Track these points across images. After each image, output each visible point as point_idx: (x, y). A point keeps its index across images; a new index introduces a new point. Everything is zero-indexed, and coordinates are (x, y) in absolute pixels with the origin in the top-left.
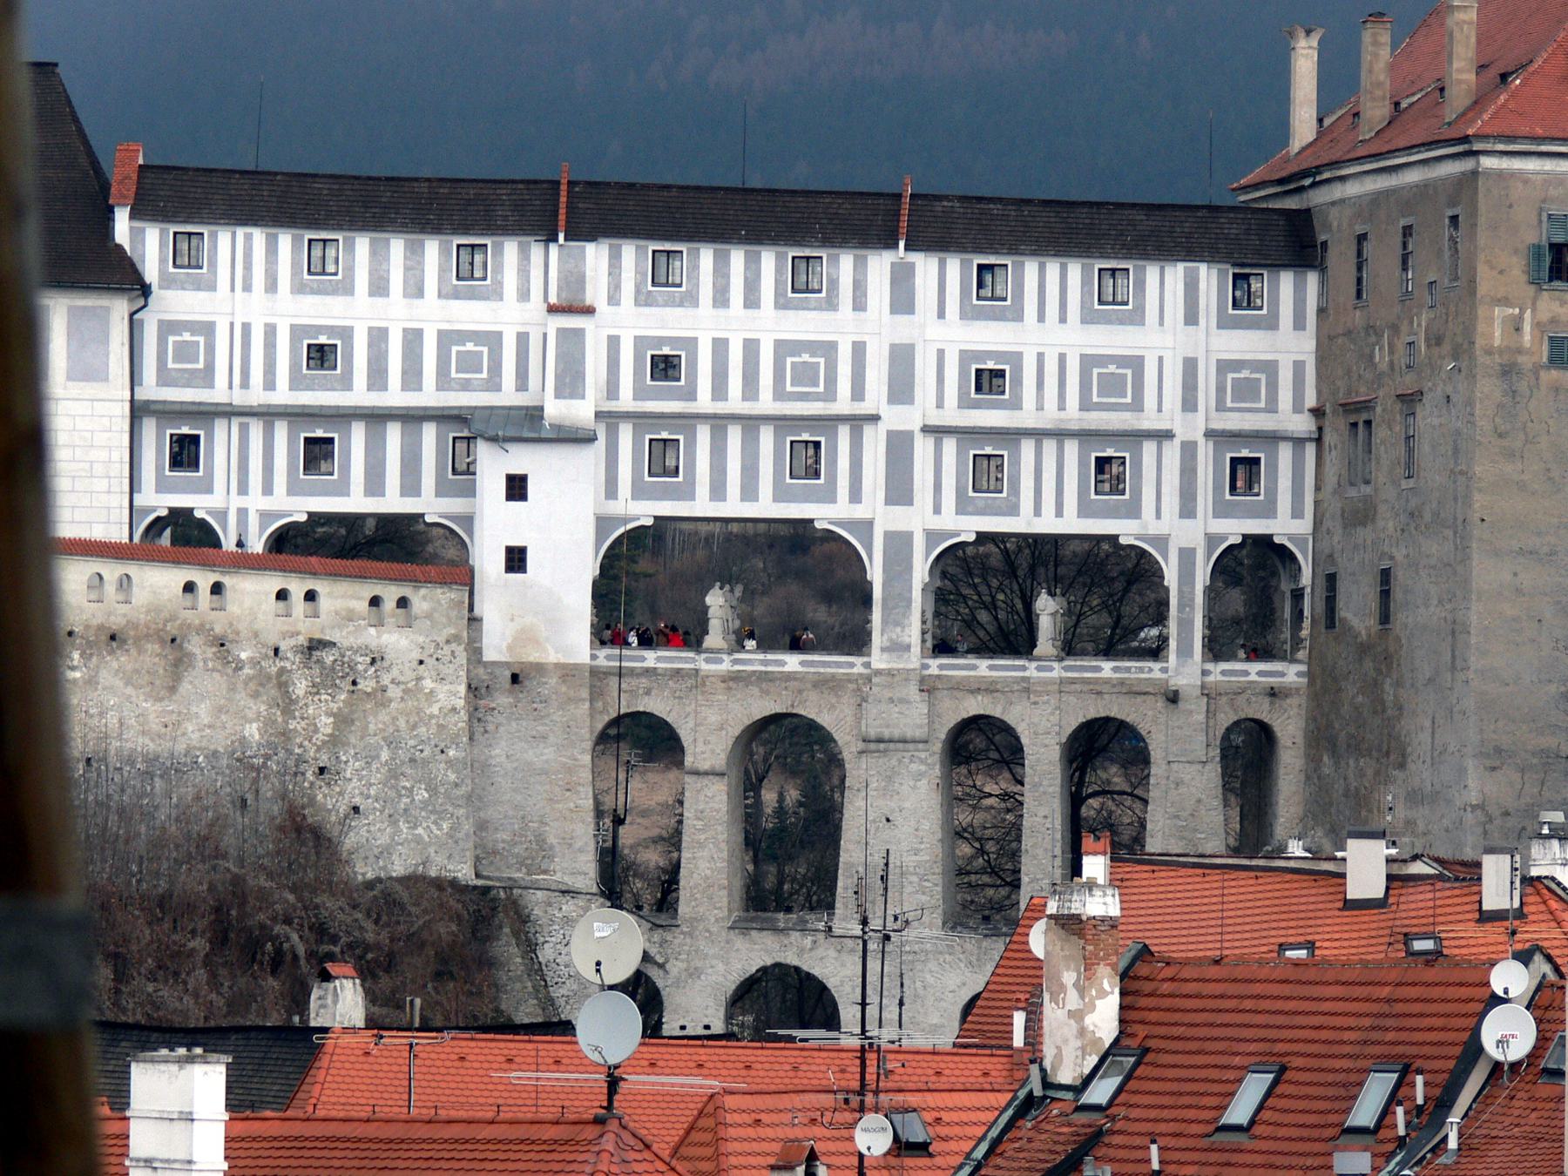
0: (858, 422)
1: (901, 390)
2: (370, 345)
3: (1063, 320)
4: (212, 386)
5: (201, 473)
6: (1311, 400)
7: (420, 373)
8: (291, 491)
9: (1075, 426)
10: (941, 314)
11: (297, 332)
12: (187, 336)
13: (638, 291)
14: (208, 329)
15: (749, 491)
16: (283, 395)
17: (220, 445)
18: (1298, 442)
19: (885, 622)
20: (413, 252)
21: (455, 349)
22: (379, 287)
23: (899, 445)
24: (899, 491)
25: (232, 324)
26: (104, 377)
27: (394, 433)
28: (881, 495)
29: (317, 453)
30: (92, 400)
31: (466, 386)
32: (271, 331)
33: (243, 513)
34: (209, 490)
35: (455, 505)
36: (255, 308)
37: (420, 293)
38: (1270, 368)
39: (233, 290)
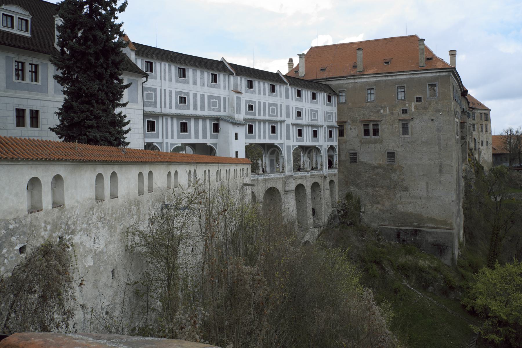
0: (282, 122)
1: (288, 116)
2: (193, 98)
3: (308, 102)
4: (156, 107)
5: (155, 132)
6: (337, 121)
7: (204, 107)
8: (178, 137)
9: (310, 124)
10: (292, 100)
11: (177, 93)
12: (149, 92)
13: (245, 89)
14: (155, 90)
15: (265, 138)
16: (174, 111)
17: (160, 125)
18: (336, 127)
19: (288, 165)
20: (202, 74)
21: (211, 100)
22: (195, 83)
23: (288, 126)
24: (288, 138)
25: (161, 89)
26: (137, 102)
27: (200, 122)
28: (285, 137)
29: (184, 128)
30: (134, 109)
31: (214, 110)
32: (170, 92)
33: (167, 143)
34: (158, 137)
35: (214, 141)
36: (166, 85)
37: (204, 85)
38: (332, 113)
39: (161, 79)
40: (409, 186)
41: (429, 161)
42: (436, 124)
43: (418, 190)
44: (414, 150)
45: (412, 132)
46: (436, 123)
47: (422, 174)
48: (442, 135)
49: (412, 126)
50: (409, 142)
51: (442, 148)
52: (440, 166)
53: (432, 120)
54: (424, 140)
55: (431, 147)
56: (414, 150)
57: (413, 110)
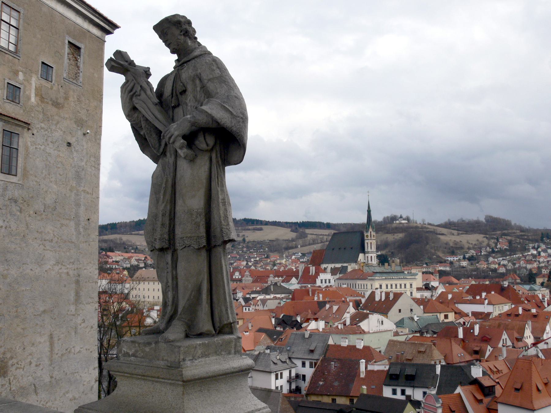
40: (8, 355)
41: (57, 268)
42: (76, 159)
43: (30, 363)
44: (28, 228)
45: (25, 169)
46: (75, 154)
47: (42, 309)
48: (82, 193)
49: (27, 149)
50: (16, 201)
51: (81, 230)
52: (77, 282)
53: (69, 144)
54: (49, 200)
55: (62, 225)
56: (28, 228)
57: (33, 99)
